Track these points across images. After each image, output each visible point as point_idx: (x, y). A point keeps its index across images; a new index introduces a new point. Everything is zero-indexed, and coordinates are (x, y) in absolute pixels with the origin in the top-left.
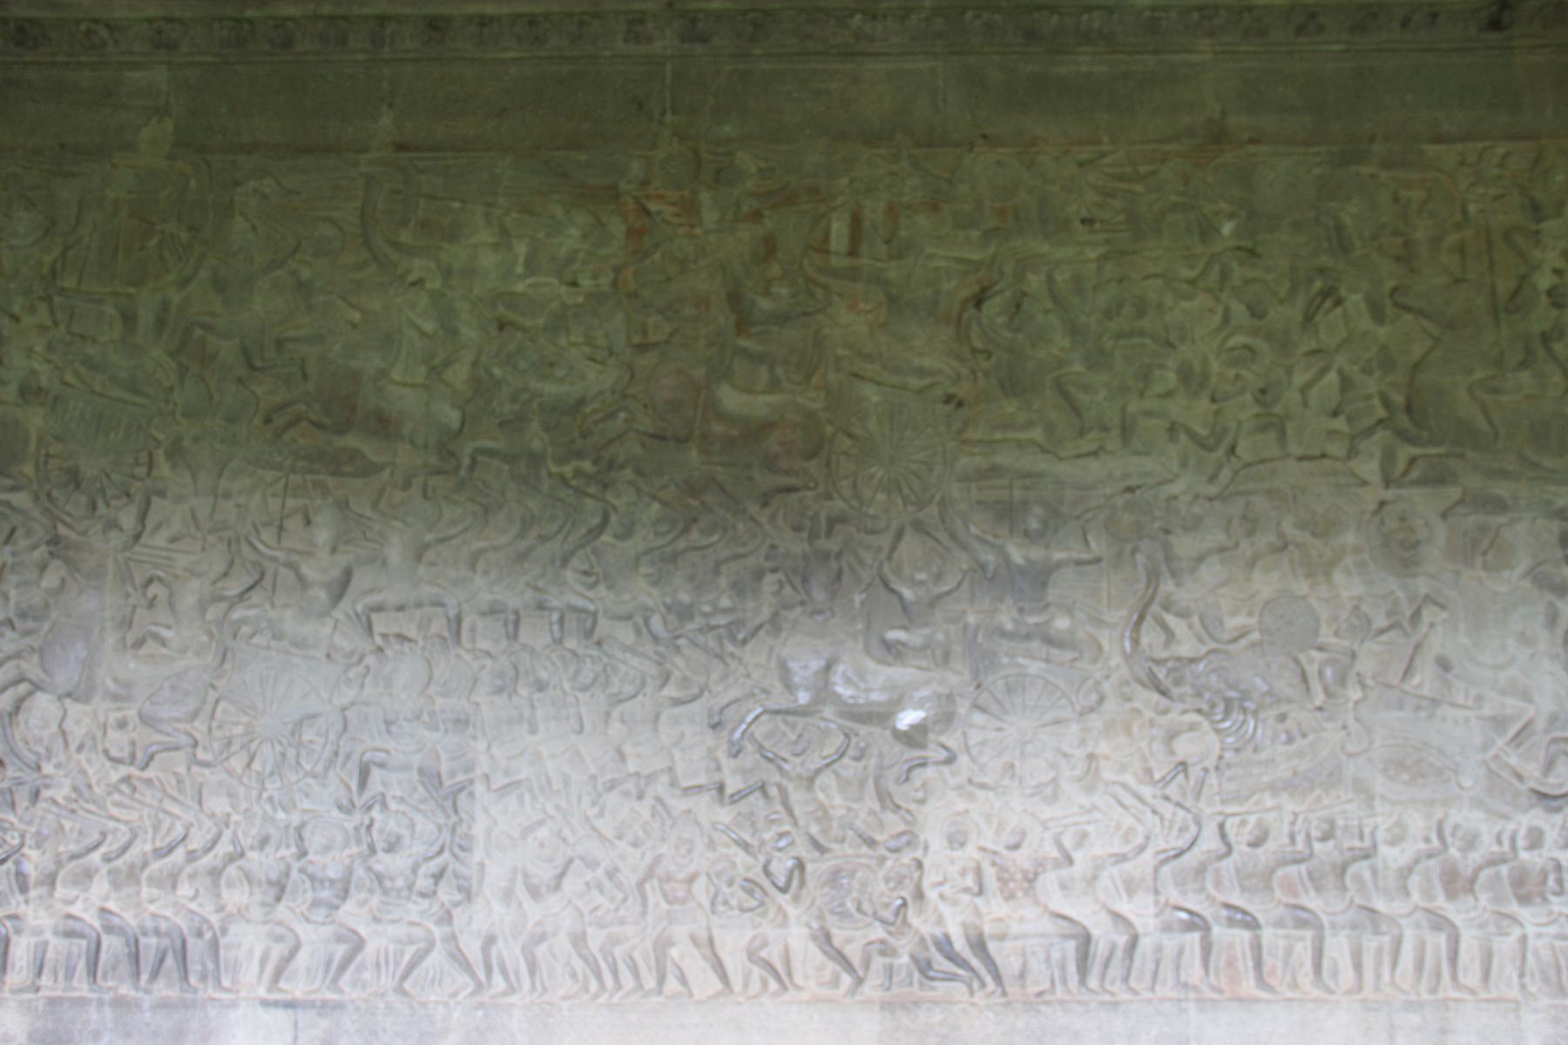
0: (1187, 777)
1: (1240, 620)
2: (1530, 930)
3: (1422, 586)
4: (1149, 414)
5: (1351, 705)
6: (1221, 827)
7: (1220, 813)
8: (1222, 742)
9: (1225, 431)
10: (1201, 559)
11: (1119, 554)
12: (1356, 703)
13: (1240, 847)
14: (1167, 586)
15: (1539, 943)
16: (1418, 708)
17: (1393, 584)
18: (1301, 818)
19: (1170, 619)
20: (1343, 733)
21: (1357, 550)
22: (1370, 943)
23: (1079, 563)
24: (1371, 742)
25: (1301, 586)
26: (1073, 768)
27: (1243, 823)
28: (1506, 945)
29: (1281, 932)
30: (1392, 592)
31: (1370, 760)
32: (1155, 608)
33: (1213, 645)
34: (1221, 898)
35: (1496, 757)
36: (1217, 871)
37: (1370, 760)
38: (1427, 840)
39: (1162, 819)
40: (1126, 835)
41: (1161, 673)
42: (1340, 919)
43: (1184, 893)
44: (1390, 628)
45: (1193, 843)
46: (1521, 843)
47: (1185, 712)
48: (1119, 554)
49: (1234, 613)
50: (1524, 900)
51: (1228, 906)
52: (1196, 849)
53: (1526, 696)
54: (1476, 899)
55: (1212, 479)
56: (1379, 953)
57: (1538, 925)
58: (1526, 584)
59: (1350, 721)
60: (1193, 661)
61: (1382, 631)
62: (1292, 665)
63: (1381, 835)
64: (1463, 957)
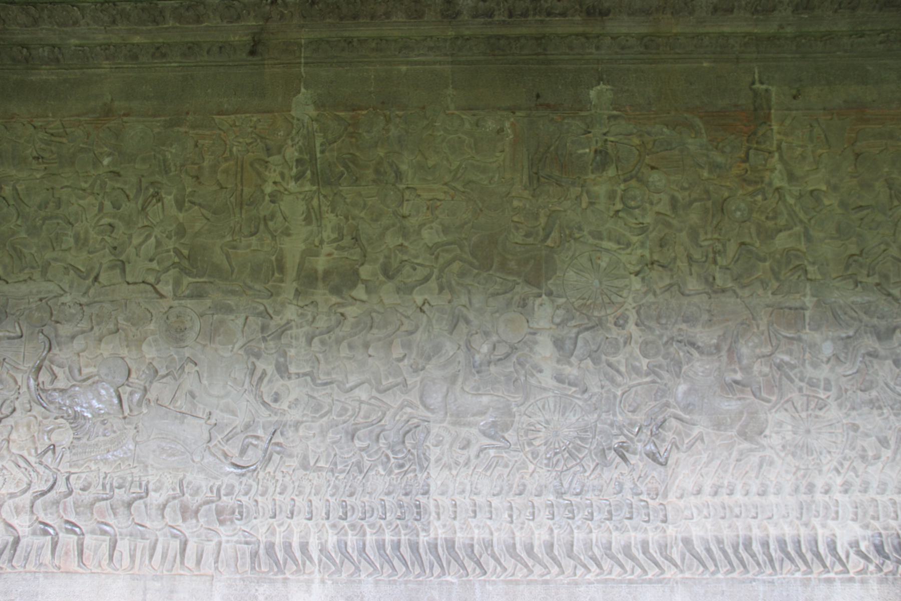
2: (224, 539)
3: (187, 353)
4: (56, 260)
6: (68, 479)
9: (92, 269)
10: (73, 337)
13: (77, 491)
14: (55, 350)
15: (228, 545)
17: (172, 351)
19: (55, 368)
22: (141, 544)
23: (9, 338)
25: (124, 352)
27: (79, 478)
28: (210, 547)
29: (95, 536)
32: (47, 362)
33: (74, 383)
34: (66, 518)
35: (216, 445)
36: (65, 503)
38: (174, 489)
39: (38, 473)
42: (124, 531)
43: (46, 514)
44: (167, 375)
45: (52, 488)
46: (223, 492)
47: (56, 418)
48: (32, 333)
49: (86, 366)
50: (222, 523)
51: (67, 522)
52: (53, 492)
53: (234, 413)
54: (198, 521)
55: (85, 293)
56: (144, 548)
57: (227, 536)
58: (241, 352)
61: (164, 377)
63: (151, 487)
64: (188, 551)
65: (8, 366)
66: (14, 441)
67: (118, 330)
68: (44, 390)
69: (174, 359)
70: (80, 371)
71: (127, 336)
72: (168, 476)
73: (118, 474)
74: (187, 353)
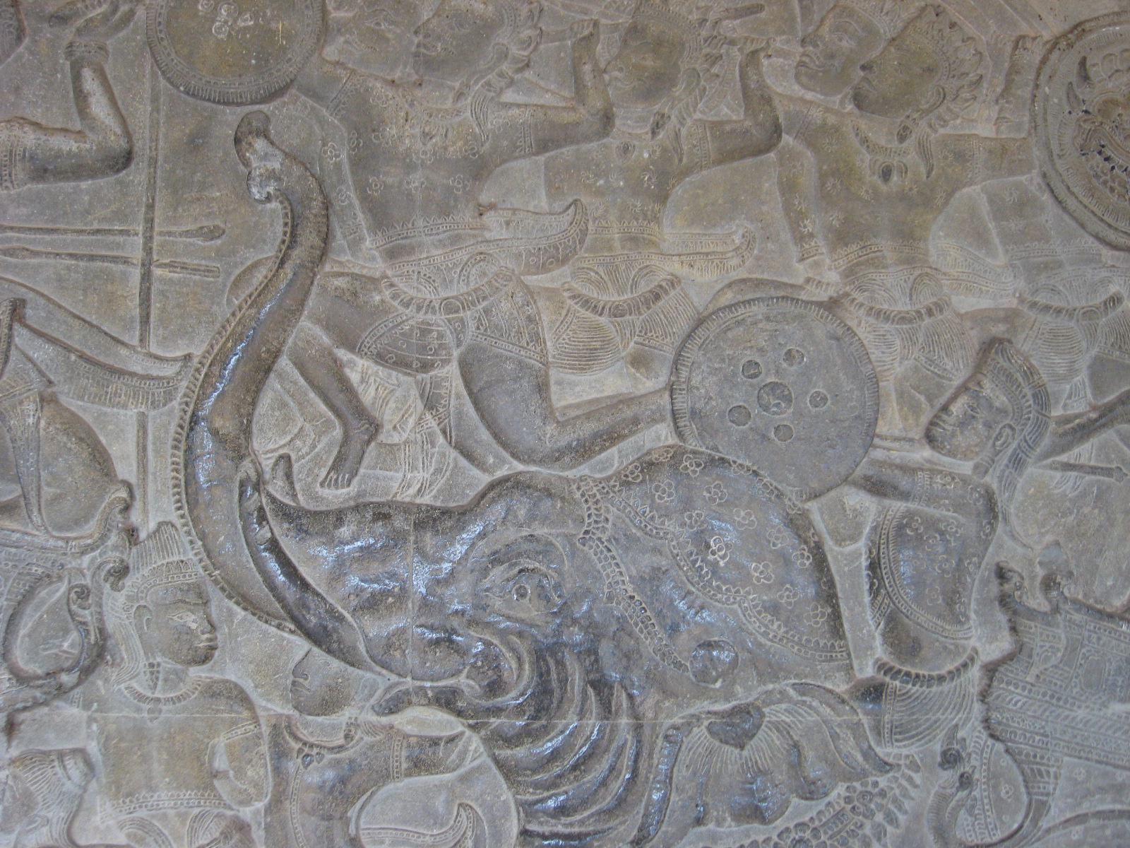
1: (610, 381)
5: (975, 673)
8: (528, 810)
10: (479, 168)
11: (195, 143)
12: (991, 670)
14: (359, 254)
19: (359, 369)
23: (43, 169)
24: (1038, 809)
25: (824, 273)
41: (314, 559)
47: (395, 705)
48: (195, 143)
49: (586, 359)
59: (972, 734)
60: (437, 520)
61: (1084, 430)
62: (785, 540)
65: (42, 353)
67: (777, 130)
71: (839, 174)
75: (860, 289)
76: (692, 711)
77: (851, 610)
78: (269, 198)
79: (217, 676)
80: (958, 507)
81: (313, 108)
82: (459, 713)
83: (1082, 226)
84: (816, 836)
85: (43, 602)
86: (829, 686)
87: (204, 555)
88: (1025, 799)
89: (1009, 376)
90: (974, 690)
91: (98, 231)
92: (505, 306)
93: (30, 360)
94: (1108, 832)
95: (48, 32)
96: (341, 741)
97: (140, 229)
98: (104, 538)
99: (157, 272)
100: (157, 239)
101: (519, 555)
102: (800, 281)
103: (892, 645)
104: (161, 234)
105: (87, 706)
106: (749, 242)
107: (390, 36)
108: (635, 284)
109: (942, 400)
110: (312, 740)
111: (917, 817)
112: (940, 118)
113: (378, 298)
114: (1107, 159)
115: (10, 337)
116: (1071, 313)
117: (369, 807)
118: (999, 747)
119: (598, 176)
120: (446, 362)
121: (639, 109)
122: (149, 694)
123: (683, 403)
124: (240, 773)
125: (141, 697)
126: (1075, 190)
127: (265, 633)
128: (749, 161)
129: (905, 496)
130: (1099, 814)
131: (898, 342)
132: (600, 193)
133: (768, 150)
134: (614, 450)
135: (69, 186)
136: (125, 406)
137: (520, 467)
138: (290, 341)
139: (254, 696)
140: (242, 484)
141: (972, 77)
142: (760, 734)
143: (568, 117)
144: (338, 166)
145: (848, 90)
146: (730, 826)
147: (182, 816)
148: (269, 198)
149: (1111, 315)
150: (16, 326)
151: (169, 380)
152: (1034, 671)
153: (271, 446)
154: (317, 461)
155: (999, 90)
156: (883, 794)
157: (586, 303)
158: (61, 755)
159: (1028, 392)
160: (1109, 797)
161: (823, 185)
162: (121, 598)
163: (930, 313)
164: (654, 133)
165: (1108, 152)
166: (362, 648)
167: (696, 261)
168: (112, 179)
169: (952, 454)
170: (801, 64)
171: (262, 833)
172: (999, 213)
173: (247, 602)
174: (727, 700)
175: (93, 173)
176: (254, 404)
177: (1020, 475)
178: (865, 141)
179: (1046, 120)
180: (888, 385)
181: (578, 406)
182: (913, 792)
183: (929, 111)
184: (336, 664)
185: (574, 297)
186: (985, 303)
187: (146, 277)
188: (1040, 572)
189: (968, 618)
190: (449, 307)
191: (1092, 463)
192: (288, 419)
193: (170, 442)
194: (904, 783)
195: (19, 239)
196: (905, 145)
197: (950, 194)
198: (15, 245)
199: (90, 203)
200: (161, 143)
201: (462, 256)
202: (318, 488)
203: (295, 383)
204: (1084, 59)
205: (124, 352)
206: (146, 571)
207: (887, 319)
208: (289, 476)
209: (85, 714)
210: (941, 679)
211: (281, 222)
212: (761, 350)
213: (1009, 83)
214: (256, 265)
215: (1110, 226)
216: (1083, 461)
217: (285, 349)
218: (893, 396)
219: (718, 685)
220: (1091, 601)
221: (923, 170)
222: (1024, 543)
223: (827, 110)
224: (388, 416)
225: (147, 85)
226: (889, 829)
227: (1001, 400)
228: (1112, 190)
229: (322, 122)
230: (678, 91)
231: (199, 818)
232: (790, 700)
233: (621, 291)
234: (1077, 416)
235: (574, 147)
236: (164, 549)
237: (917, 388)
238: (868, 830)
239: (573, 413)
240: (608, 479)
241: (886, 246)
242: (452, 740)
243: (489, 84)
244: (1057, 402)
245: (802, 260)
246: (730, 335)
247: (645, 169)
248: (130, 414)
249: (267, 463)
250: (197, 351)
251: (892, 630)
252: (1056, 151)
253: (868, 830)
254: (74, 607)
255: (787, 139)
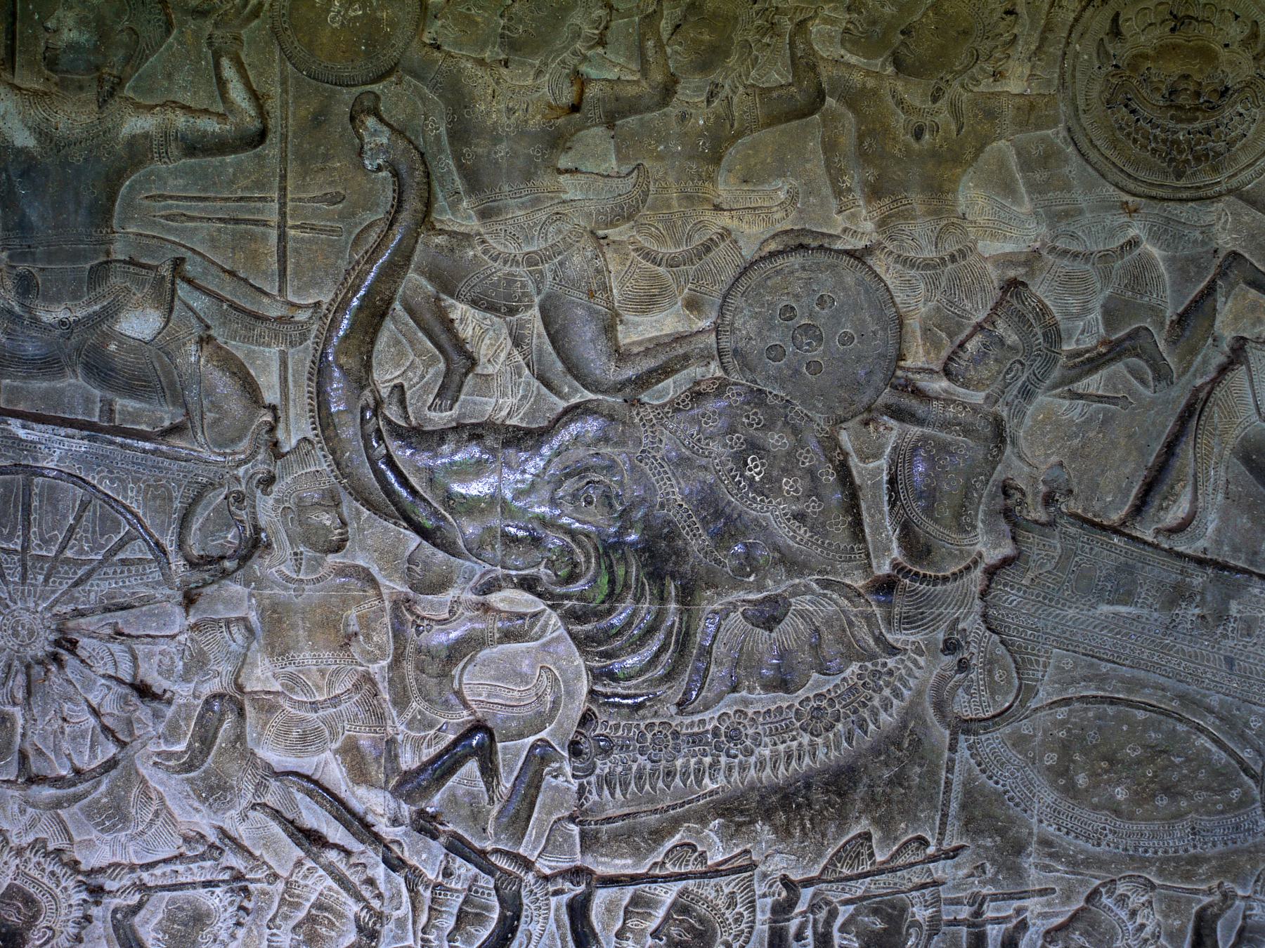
0: (489, 771)
1: (667, 322)
5: (977, 574)
6: (578, 911)
7: (576, 874)
8: (597, 675)
12: (991, 572)
16: (1178, 595)
18: (807, 894)
20: (949, 660)
21: (1030, 113)
23: (194, 146)
24: (1026, 691)
25: (858, 224)
26: (173, 733)
30: (1133, 243)
31: (1020, 742)
32: (414, 281)
37: (1020, 742)
39: (414, 879)
40: (311, 919)
44: (1113, 352)
47: (490, 587)
48: (318, 120)
49: (647, 303)
59: (971, 623)
61: (1093, 363)
65: (200, 303)
66: (268, 707)
67: (821, 95)
68: (417, 436)
69: (1146, 264)
70: (609, 329)
72: (1136, 900)
73: (859, 888)
74: (1225, 227)
75: (891, 239)
76: (730, 599)
77: (872, 516)
78: (379, 168)
79: (348, 561)
80: (967, 431)
81: (416, 86)
82: (540, 596)
83: (1103, 176)
84: (832, 706)
85: (210, 503)
86: (848, 582)
87: (334, 467)
88: (1016, 682)
89: (1022, 318)
90: (976, 590)
91: (241, 199)
92: (576, 259)
93: (191, 309)
94: (1091, 714)
95: (192, 24)
96: (447, 616)
97: (276, 195)
98: (253, 455)
99: (292, 232)
100: (290, 205)
101: (587, 469)
102: (838, 231)
103: (905, 548)
104: (293, 200)
105: (247, 585)
106: (793, 196)
107: (479, 20)
108: (690, 238)
109: (962, 337)
110: (424, 614)
111: (919, 693)
112: (973, 78)
113: (471, 253)
114: (1133, 112)
115: (173, 291)
116: (1087, 257)
117: (469, 668)
118: (995, 637)
119: (659, 142)
120: (531, 307)
121: (696, 79)
122: (295, 576)
123: (727, 343)
124: (368, 638)
125: (288, 579)
126: (1098, 143)
127: (386, 529)
128: (795, 123)
129: (920, 422)
130: (1082, 699)
131: (922, 286)
132: (660, 157)
133: (812, 114)
134: (670, 381)
135: (216, 160)
136: (269, 345)
137: (591, 396)
138: (401, 290)
139: (379, 577)
140: (363, 411)
141: (1007, 37)
142: (787, 619)
143: (631, 91)
144: (438, 137)
145: (888, 53)
146: (759, 694)
147: (322, 673)
148: (379, 168)
149: (1127, 258)
150: (178, 281)
151: (302, 324)
152: (1030, 575)
153: (388, 377)
154: (426, 389)
155: (1033, 47)
156: (890, 673)
157: (647, 255)
158: (228, 623)
159: (1038, 330)
160: (1093, 685)
161: (861, 143)
162: (270, 501)
163: (953, 258)
164: (709, 102)
165: (1134, 106)
166: (460, 542)
167: (749, 216)
168: (251, 153)
169: (963, 385)
170: (846, 31)
171: (386, 684)
172: (1027, 165)
173: (368, 503)
174: (760, 591)
175: (235, 150)
176: (373, 342)
177: (1030, 403)
178: (900, 103)
179: (1074, 77)
180: (914, 324)
181: (640, 343)
182: (917, 672)
183: (966, 68)
184: (441, 555)
185: (637, 250)
186: (1009, 247)
187: (282, 237)
188: (1042, 488)
189: (975, 527)
190: (531, 260)
191: (1100, 393)
192: (402, 354)
193: (306, 375)
194: (911, 665)
195: (178, 206)
196: (938, 104)
197: (979, 150)
198: (175, 211)
199: (234, 175)
200: (290, 121)
201: (542, 216)
202: (427, 412)
203: (406, 324)
204: (1117, 14)
205: (266, 300)
206: (289, 480)
207: (912, 266)
208: (402, 402)
209: (247, 590)
210: (945, 579)
211: (391, 187)
212: (797, 296)
213: (1043, 40)
214: (371, 226)
215: (1129, 176)
216: (1091, 390)
217: (397, 296)
218: (918, 333)
219: (752, 579)
220: (1090, 515)
221: (953, 127)
222: (1030, 462)
223: (868, 73)
224: (483, 351)
225: (277, 70)
226: (895, 701)
227: (1012, 338)
228: (1135, 141)
229: (423, 99)
230: (732, 61)
231: (337, 673)
232: (813, 593)
233: (677, 243)
234: (1087, 351)
235: (638, 117)
236: (303, 462)
237: (939, 327)
238: (876, 702)
239: (635, 350)
240: (663, 406)
241: (916, 200)
242: (535, 615)
243: (563, 62)
244: (1070, 337)
245: (840, 212)
246: (769, 283)
247: (701, 135)
248: (273, 351)
249: (385, 392)
250: (326, 299)
251: (905, 536)
252: (1082, 106)
253: (876, 702)
254: (233, 508)
255: (830, 101)
